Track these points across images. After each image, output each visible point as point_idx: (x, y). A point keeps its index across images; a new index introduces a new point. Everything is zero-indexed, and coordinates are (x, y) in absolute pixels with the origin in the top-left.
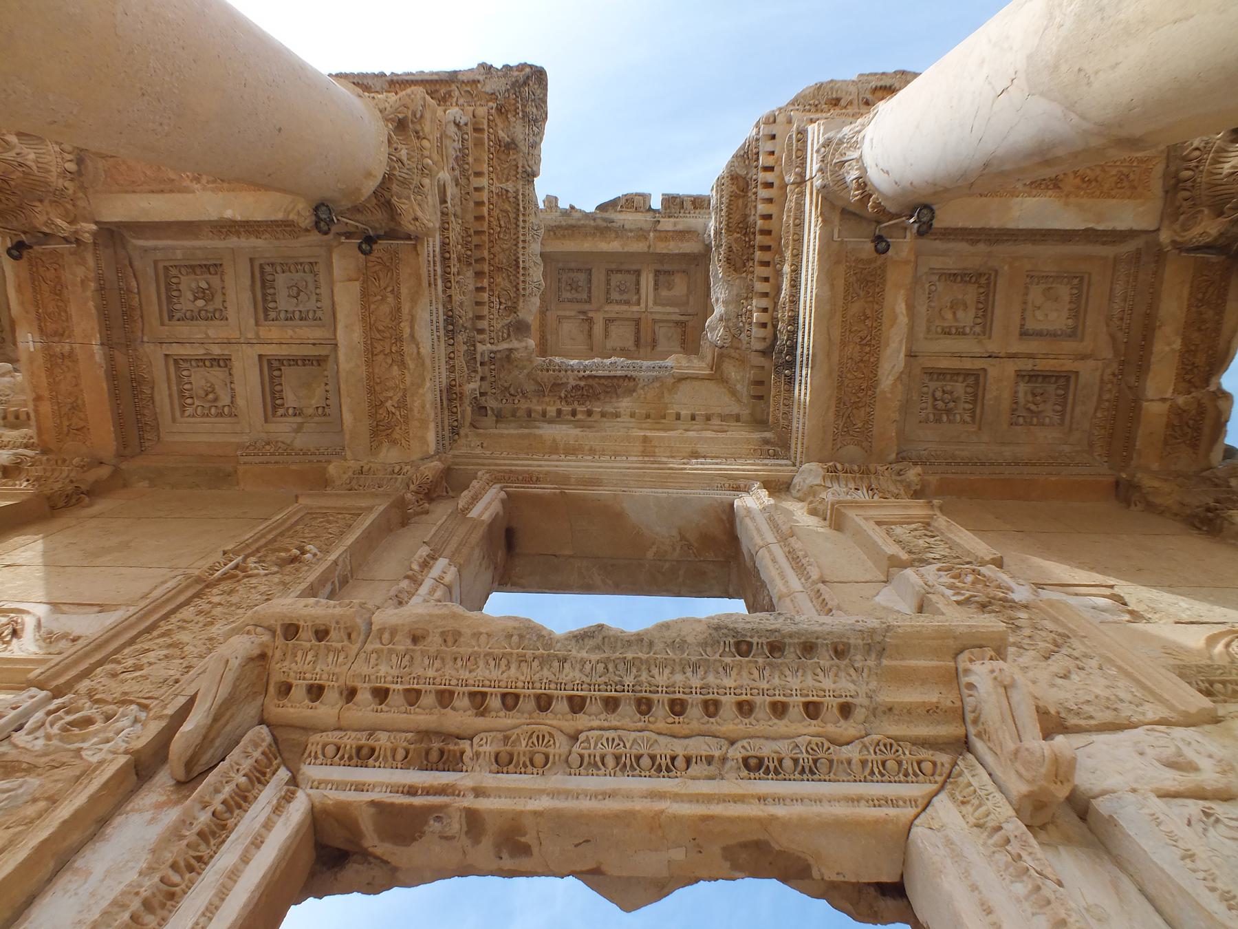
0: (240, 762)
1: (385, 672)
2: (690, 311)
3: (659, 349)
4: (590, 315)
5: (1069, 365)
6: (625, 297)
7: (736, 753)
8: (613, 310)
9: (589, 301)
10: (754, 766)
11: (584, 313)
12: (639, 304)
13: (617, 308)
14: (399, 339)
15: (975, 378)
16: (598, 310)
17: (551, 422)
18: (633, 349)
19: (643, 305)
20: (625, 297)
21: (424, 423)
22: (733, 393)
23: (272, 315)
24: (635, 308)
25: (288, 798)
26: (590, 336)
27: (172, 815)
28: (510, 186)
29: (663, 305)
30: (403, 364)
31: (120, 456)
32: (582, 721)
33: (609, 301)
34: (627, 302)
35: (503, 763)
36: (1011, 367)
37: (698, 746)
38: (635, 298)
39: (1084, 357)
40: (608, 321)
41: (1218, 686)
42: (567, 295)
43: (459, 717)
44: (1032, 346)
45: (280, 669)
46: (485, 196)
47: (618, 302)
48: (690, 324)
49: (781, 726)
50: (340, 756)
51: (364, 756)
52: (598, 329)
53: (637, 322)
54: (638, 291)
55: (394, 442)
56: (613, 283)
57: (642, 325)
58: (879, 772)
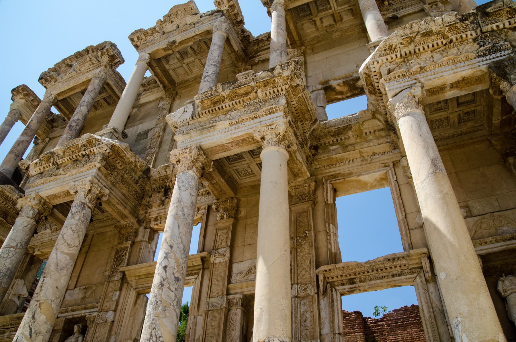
0: (329, 290)
1: (341, 273)
2: (352, 4)
3: (344, 20)
4: (314, 19)
5: (473, 109)
6: (325, 7)
7: (391, 274)
8: (322, 14)
9: (311, 14)
10: (393, 276)
11: (311, 19)
12: (331, 8)
13: (323, 13)
14: (294, 160)
15: (447, 118)
16: (316, 16)
17: (332, 145)
18: (334, 23)
19: (333, 9)
20: (325, 7)
21: (306, 172)
22: (380, 121)
23: (255, 154)
24: (330, 11)
25: (337, 293)
26: (315, 25)
27: (325, 299)
28: (300, 95)
29: (341, 6)
30: (297, 164)
31: (235, 194)
32: (369, 274)
33: (319, 11)
34: (326, 9)
35: (361, 282)
36: (456, 114)
37: (386, 274)
38: (329, 6)
39: (478, 106)
40: (321, 19)
42: (302, 15)
43: (353, 276)
44: (462, 108)
45: (327, 276)
46: (296, 105)
47: (323, 10)
48: (354, 9)
49: (396, 269)
50: (339, 285)
51: (343, 284)
52: (318, 23)
53: (333, 15)
54: (329, 4)
55: (300, 177)
56: (318, 4)
57: (335, 16)
58: (410, 274)
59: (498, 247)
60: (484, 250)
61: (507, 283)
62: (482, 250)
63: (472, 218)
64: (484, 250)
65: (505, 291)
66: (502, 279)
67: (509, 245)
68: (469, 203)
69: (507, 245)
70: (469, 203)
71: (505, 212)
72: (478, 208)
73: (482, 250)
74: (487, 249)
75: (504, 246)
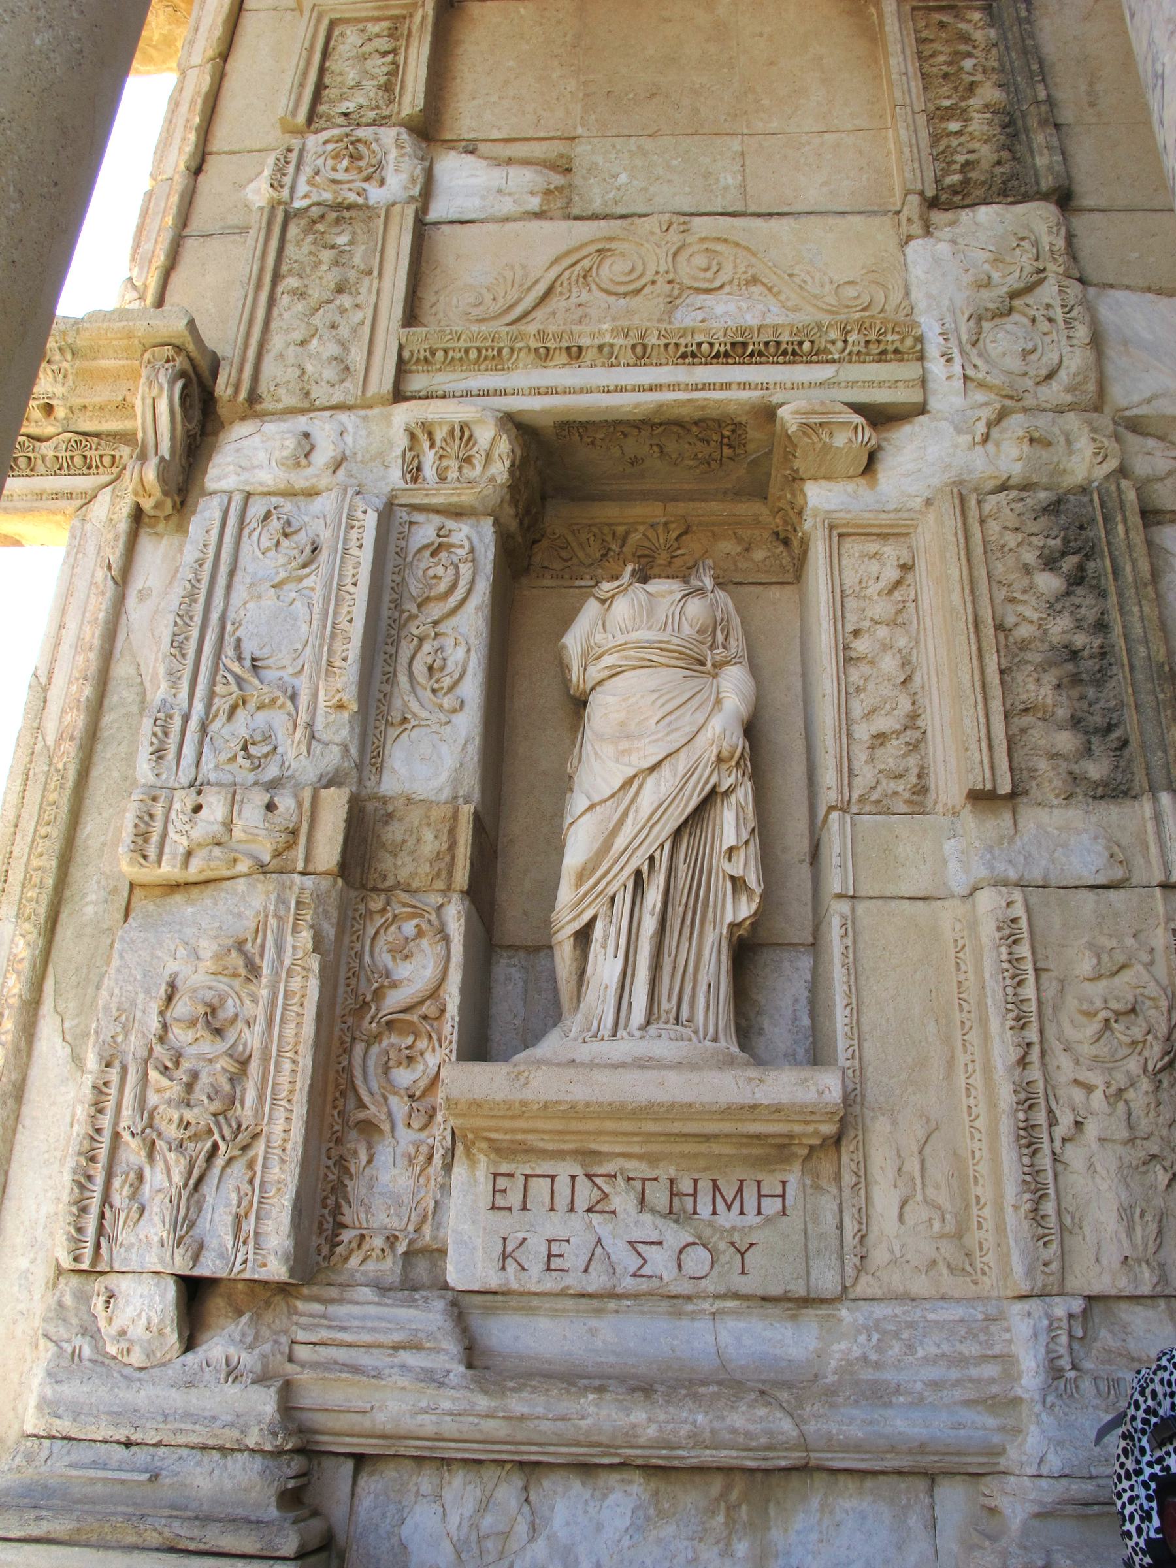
41: (440, 355)
59: (640, 388)
60: (550, 391)
61: (622, 608)
62: (538, 392)
63: (565, 225)
64: (550, 391)
65: (590, 656)
66: (606, 586)
67: (706, 386)
68: (581, 149)
69: (696, 388)
70: (581, 149)
71: (759, 222)
72: (623, 178)
73: (538, 392)
74: (568, 391)
75: (674, 387)
